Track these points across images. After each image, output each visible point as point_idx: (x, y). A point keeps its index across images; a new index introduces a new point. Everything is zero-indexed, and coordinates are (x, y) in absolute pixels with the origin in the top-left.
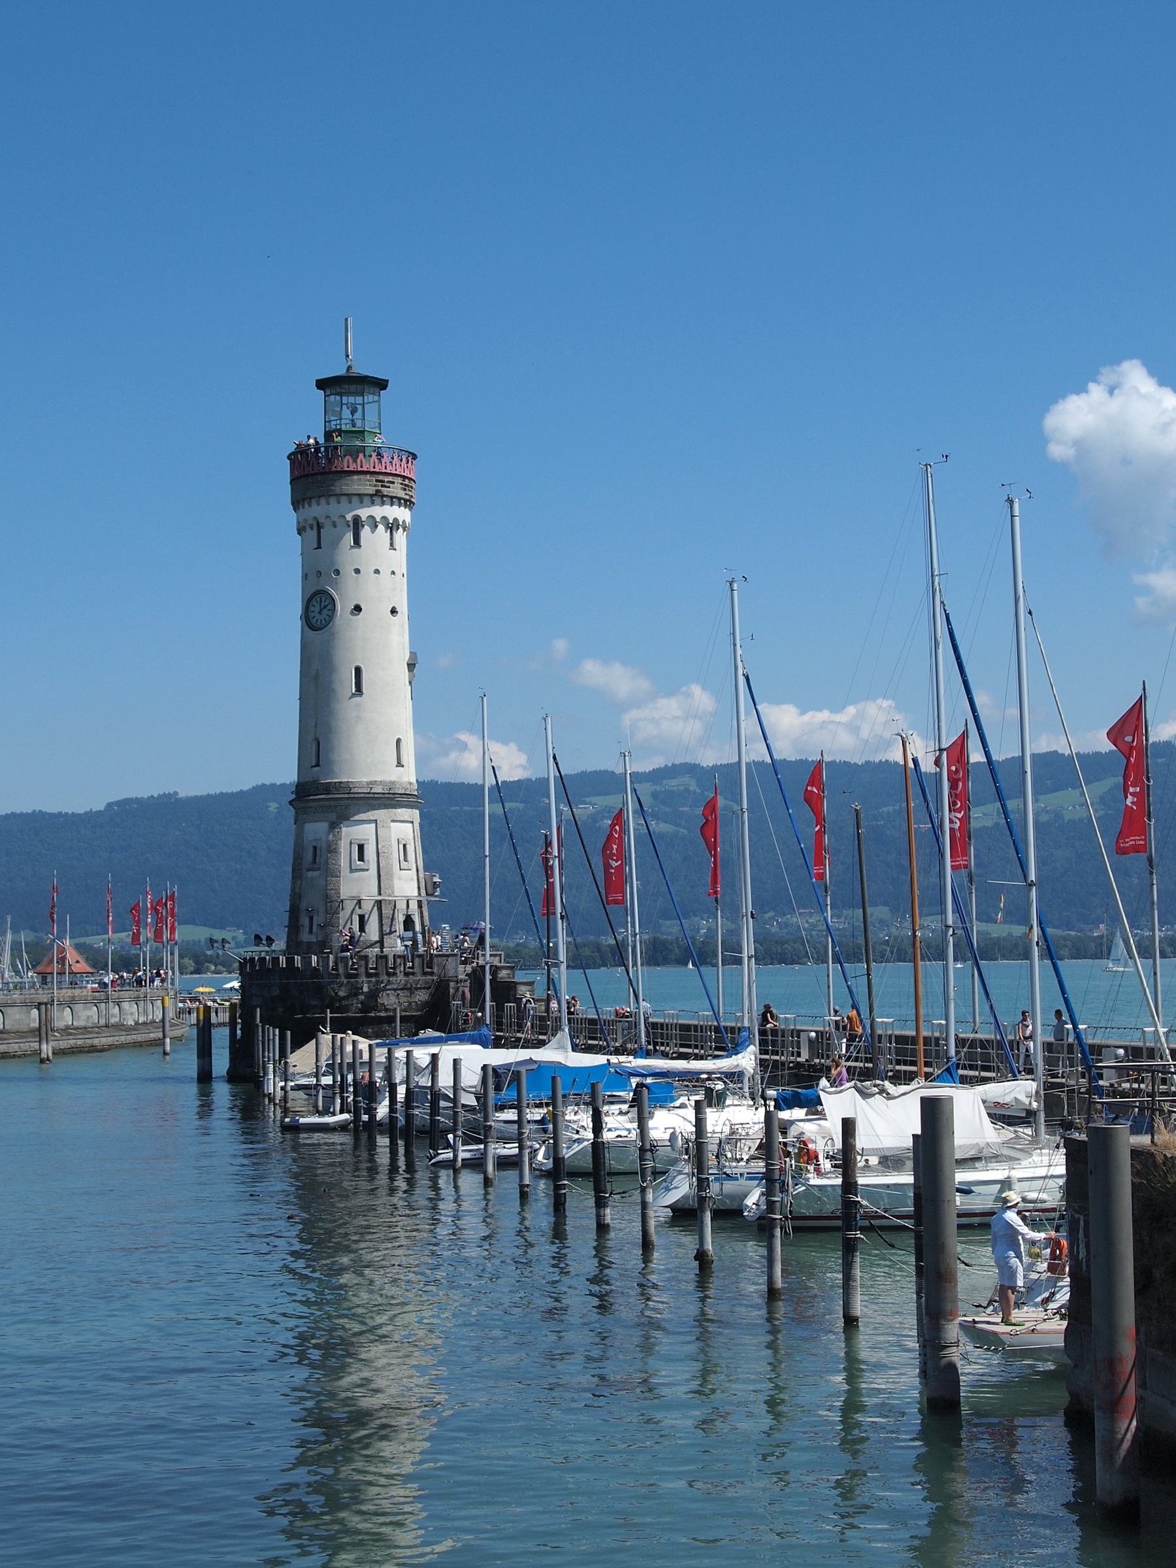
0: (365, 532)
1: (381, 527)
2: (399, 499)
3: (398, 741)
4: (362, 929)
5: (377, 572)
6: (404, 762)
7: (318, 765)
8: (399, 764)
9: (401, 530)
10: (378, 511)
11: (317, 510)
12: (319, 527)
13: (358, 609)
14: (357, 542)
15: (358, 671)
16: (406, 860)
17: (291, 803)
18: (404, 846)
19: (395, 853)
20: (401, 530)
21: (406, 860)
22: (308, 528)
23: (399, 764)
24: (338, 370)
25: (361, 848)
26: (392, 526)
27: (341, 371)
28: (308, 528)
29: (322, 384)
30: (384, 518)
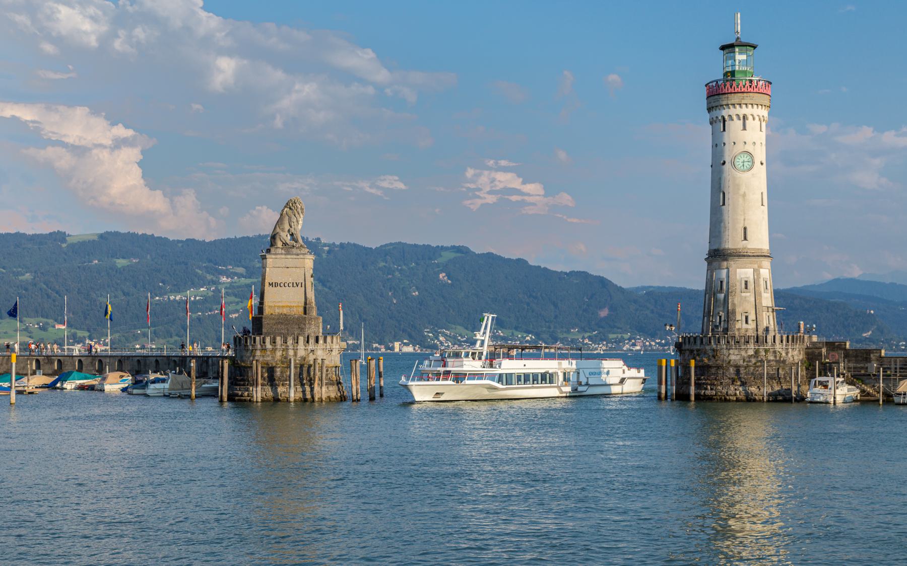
3: (745, 229)
6: (748, 237)
10: (732, 111)
13: (724, 163)
15: (724, 194)
16: (746, 288)
17: (706, 259)
18: (746, 282)
19: (740, 286)
21: (746, 288)
23: (745, 239)
24: (732, 41)
25: (722, 282)
27: (733, 41)
29: (723, 48)
30: (738, 115)
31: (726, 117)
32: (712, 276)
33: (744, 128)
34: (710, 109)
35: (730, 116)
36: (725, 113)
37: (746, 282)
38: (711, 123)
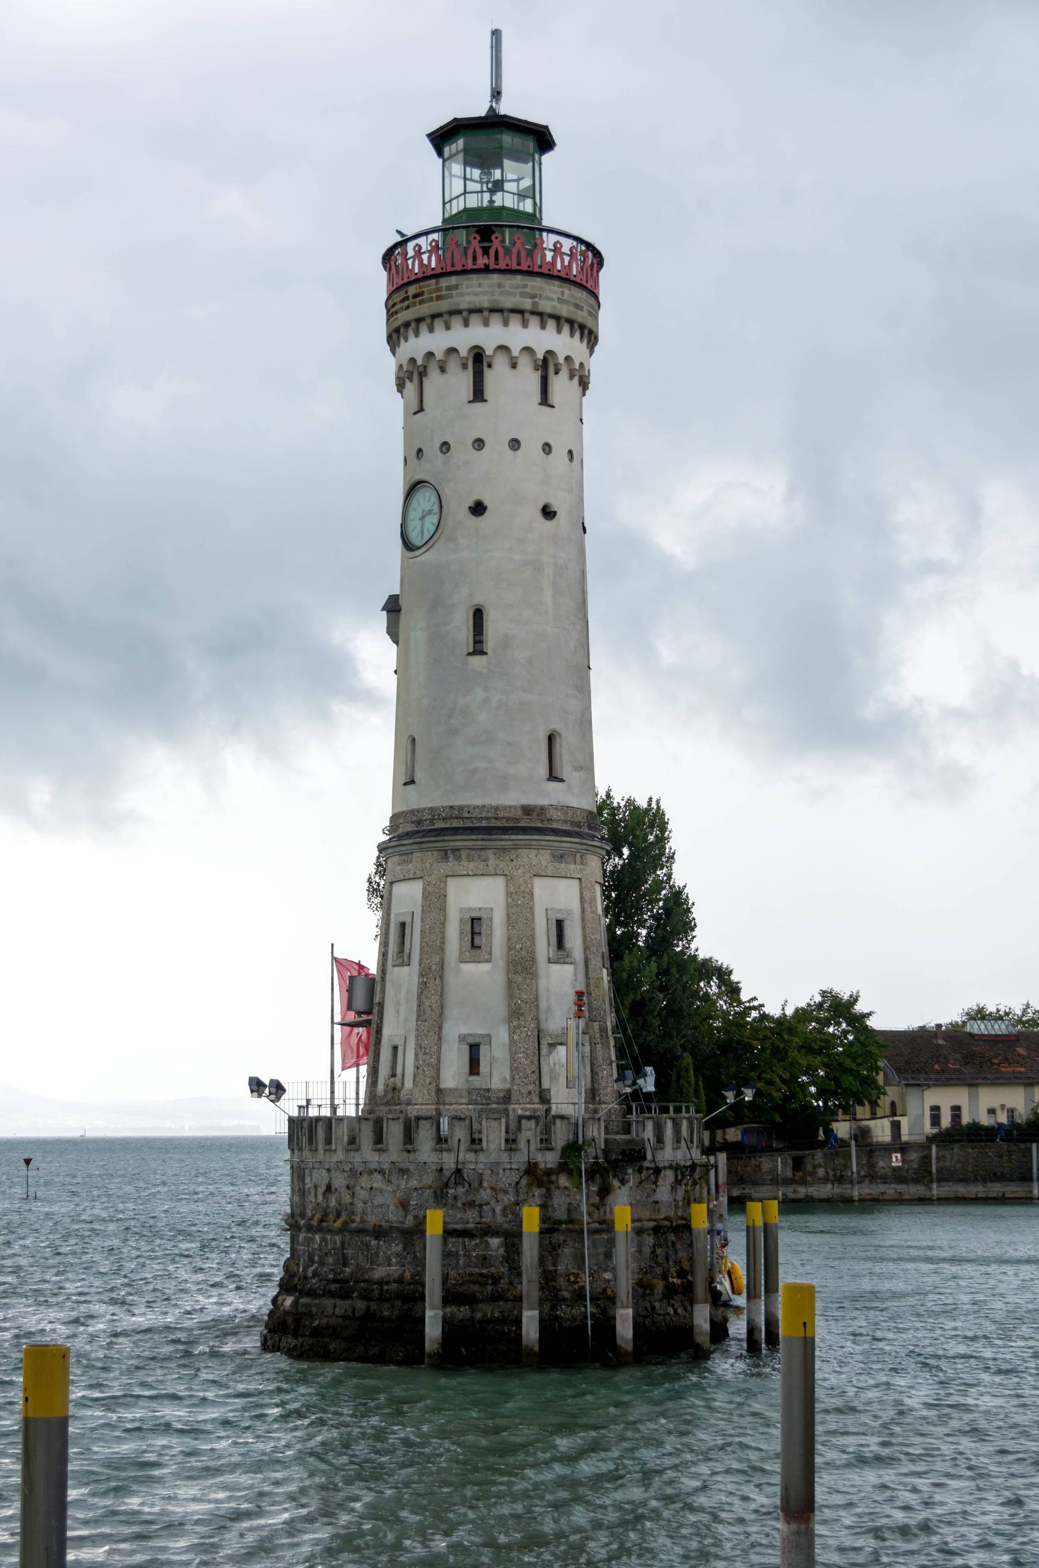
0: (497, 377)
1: (525, 366)
2: (557, 318)
3: (551, 738)
4: (474, 1067)
5: (515, 444)
7: (412, 782)
8: (553, 776)
9: (564, 372)
11: (417, 345)
12: (423, 373)
13: (478, 509)
14: (479, 394)
15: (478, 615)
20: (564, 372)
22: (407, 381)
26: (546, 365)
28: (407, 381)
29: (440, 139)
30: (528, 350)
31: (489, 352)
32: (435, 901)
33: (545, 399)
34: (395, 337)
35: (503, 348)
36: (488, 335)
37: (560, 924)
38: (412, 376)
